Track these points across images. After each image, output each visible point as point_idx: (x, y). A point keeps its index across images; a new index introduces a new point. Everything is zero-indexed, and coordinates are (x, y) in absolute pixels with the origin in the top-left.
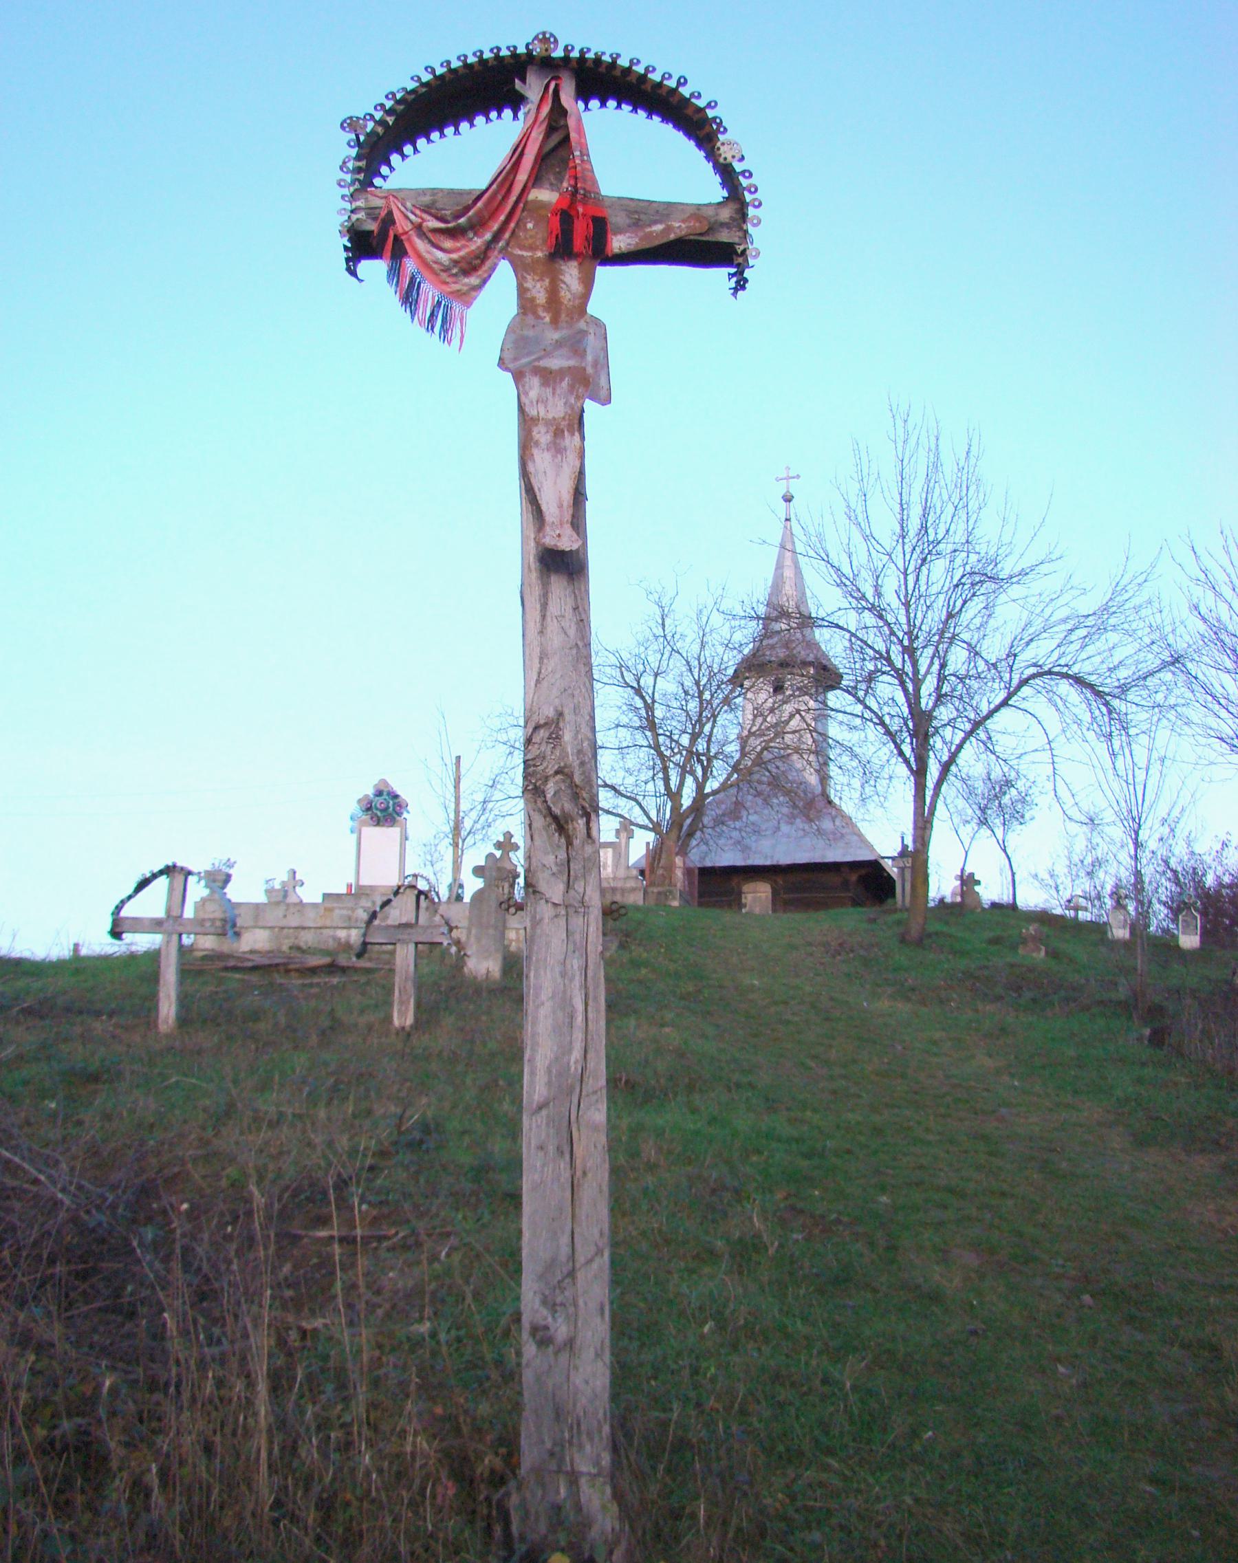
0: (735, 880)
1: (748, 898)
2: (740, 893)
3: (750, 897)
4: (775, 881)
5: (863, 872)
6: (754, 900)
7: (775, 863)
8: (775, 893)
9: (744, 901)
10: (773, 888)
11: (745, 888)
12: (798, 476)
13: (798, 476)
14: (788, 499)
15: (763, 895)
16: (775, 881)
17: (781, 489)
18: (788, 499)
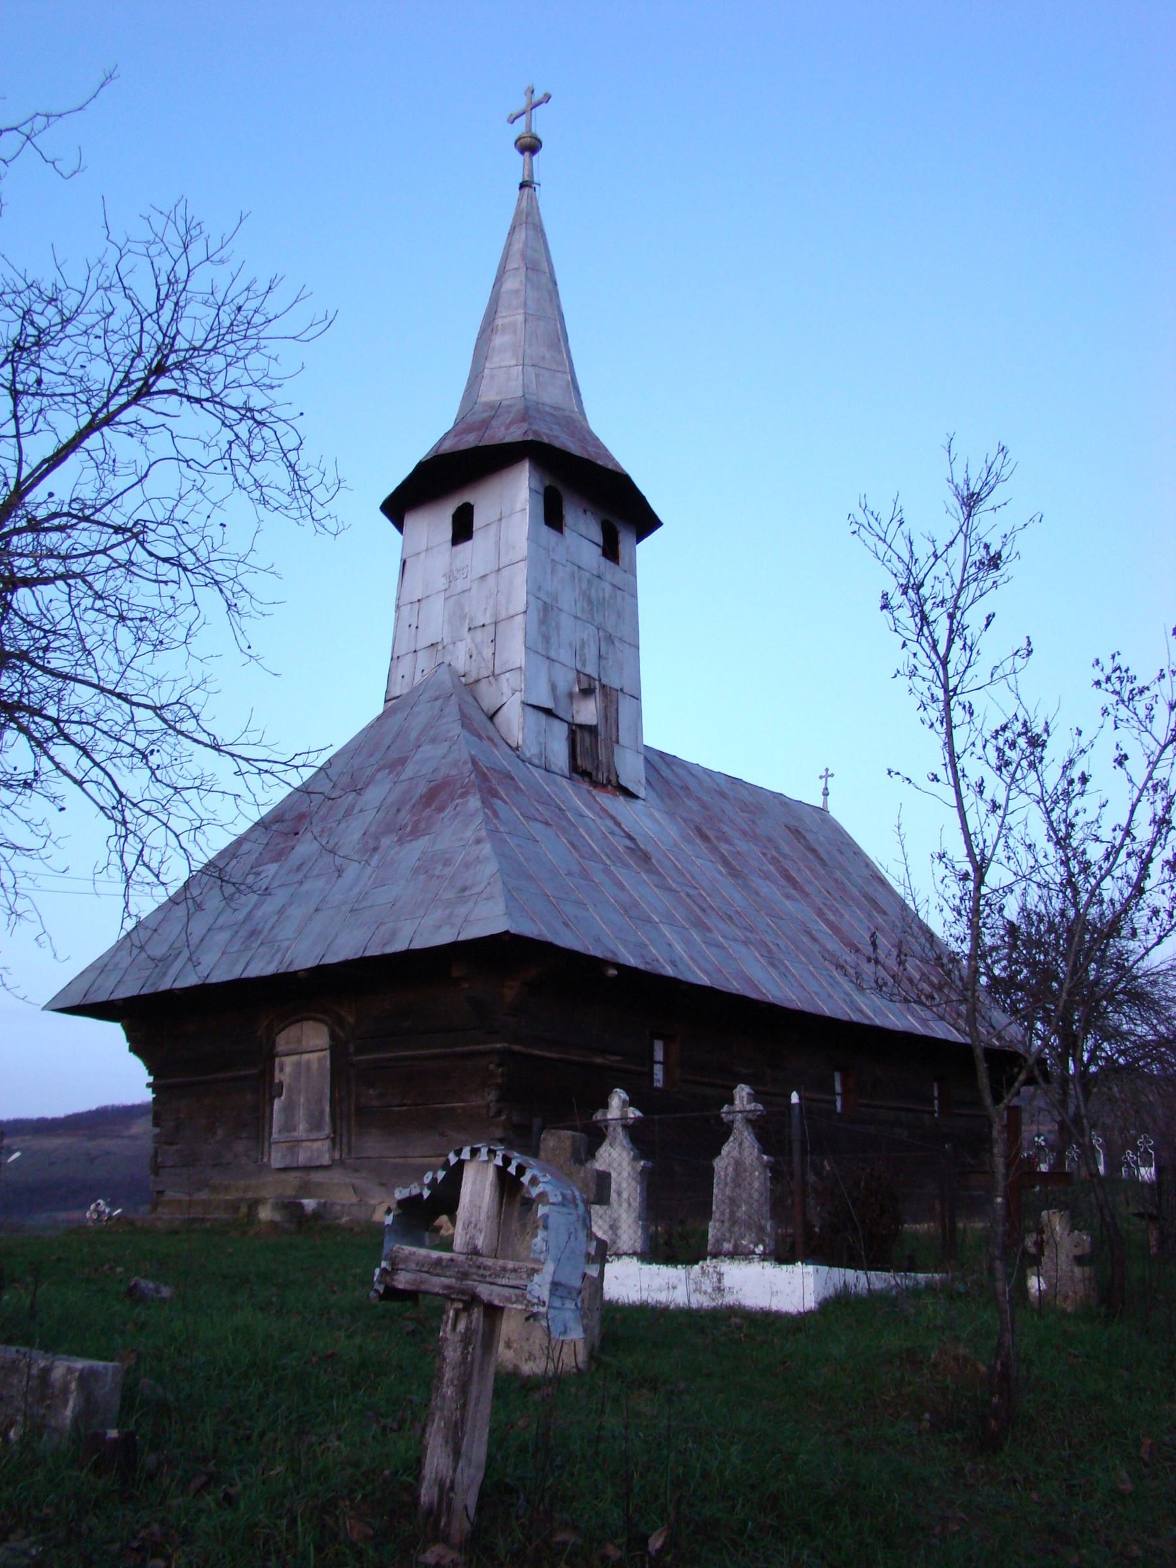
1: (286, 1069)
3: (289, 1062)
8: (337, 1050)
10: (333, 1036)
11: (283, 1041)
12: (547, 98)
14: (529, 146)
17: (520, 127)
18: (529, 146)
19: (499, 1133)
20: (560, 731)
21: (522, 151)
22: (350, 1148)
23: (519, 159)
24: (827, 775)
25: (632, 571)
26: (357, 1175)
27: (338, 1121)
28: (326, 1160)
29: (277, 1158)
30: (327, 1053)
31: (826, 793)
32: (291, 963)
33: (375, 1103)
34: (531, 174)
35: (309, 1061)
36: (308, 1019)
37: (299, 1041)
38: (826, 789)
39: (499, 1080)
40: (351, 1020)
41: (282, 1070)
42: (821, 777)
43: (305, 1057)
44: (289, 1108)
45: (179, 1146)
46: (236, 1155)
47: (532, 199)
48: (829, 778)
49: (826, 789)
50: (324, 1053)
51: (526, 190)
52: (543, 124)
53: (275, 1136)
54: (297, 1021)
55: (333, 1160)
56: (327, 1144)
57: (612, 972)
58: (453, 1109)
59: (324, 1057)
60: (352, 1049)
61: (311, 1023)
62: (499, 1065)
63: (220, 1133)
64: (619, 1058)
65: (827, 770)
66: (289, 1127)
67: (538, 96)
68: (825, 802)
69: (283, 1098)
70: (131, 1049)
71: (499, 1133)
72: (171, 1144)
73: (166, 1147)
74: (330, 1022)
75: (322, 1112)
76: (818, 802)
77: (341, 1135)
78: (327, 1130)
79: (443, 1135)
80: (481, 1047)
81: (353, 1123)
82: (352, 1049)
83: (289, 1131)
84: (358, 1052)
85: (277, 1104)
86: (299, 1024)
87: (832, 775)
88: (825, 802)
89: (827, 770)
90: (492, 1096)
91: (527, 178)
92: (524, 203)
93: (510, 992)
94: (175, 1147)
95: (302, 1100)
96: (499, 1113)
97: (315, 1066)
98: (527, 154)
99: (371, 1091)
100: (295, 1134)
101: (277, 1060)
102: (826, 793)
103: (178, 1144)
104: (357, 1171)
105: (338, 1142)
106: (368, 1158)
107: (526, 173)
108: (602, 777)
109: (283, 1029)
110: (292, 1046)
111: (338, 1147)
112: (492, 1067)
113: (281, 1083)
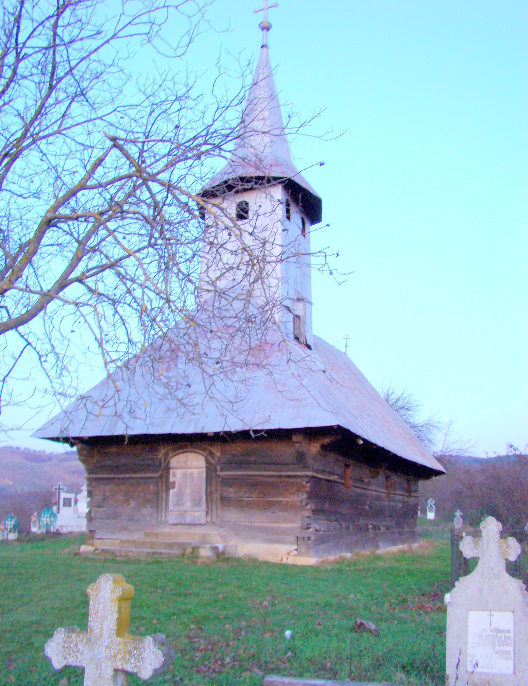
0: (163, 451)
2: (168, 468)
4: (211, 454)
5: (326, 441)
6: (185, 475)
7: (198, 431)
8: (210, 469)
9: (172, 479)
10: (207, 461)
12: (276, 5)
13: (276, 5)
14: (266, 28)
15: (195, 471)
16: (211, 454)
17: (260, 18)
18: (266, 28)
19: (307, 514)
20: (291, 317)
21: (263, 29)
22: (217, 516)
23: (261, 33)
24: (347, 338)
25: (309, 243)
26: (222, 529)
27: (210, 503)
28: (203, 521)
29: (172, 518)
30: (204, 470)
31: (346, 346)
32: (203, 428)
33: (232, 495)
34: (267, 42)
35: (192, 474)
36: (191, 452)
37: (186, 462)
38: (346, 344)
39: (308, 489)
40: (219, 454)
41: (174, 475)
42: (344, 339)
43: (189, 471)
44: (180, 495)
45: (105, 509)
46: (143, 516)
47: (267, 54)
48: (348, 340)
49: (346, 344)
50: (200, 470)
51: (265, 49)
52: (272, 17)
53: (171, 507)
54: (184, 452)
55: (207, 522)
56: (204, 513)
57: (361, 442)
58: (281, 501)
59: (202, 471)
60: (219, 468)
61: (193, 454)
62: (307, 483)
63: (133, 503)
64: (336, 477)
65: (347, 336)
66: (179, 503)
67: (270, 3)
68: (346, 350)
69: (176, 489)
70: (44, 451)
71: (307, 514)
72: (99, 507)
73: (97, 509)
74: (205, 454)
75: (200, 498)
76: (343, 350)
77: (212, 511)
78: (204, 507)
79: (273, 512)
80: (298, 473)
81: (219, 504)
82: (219, 468)
83: (179, 505)
84: (222, 470)
85: (172, 492)
86: (186, 454)
87: (350, 338)
88: (346, 350)
89: (347, 336)
90: (305, 496)
91: (265, 43)
92: (264, 56)
93: (314, 448)
94: (102, 509)
95: (188, 491)
96: (307, 504)
97: (196, 475)
98: (265, 31)
99: (230, 489)
100: (184, 507)
101: (171, 471)
102: (346, 346)
103: (103, 507)
104: (222, 527)
105: (210, 512)
106: (229, 521)
107: (265, 40)
108: (302, 340)
109: (174, 456)
110: (183, 465)
111: (210, 515)
112: (304, 483)
113: (174, 483)
